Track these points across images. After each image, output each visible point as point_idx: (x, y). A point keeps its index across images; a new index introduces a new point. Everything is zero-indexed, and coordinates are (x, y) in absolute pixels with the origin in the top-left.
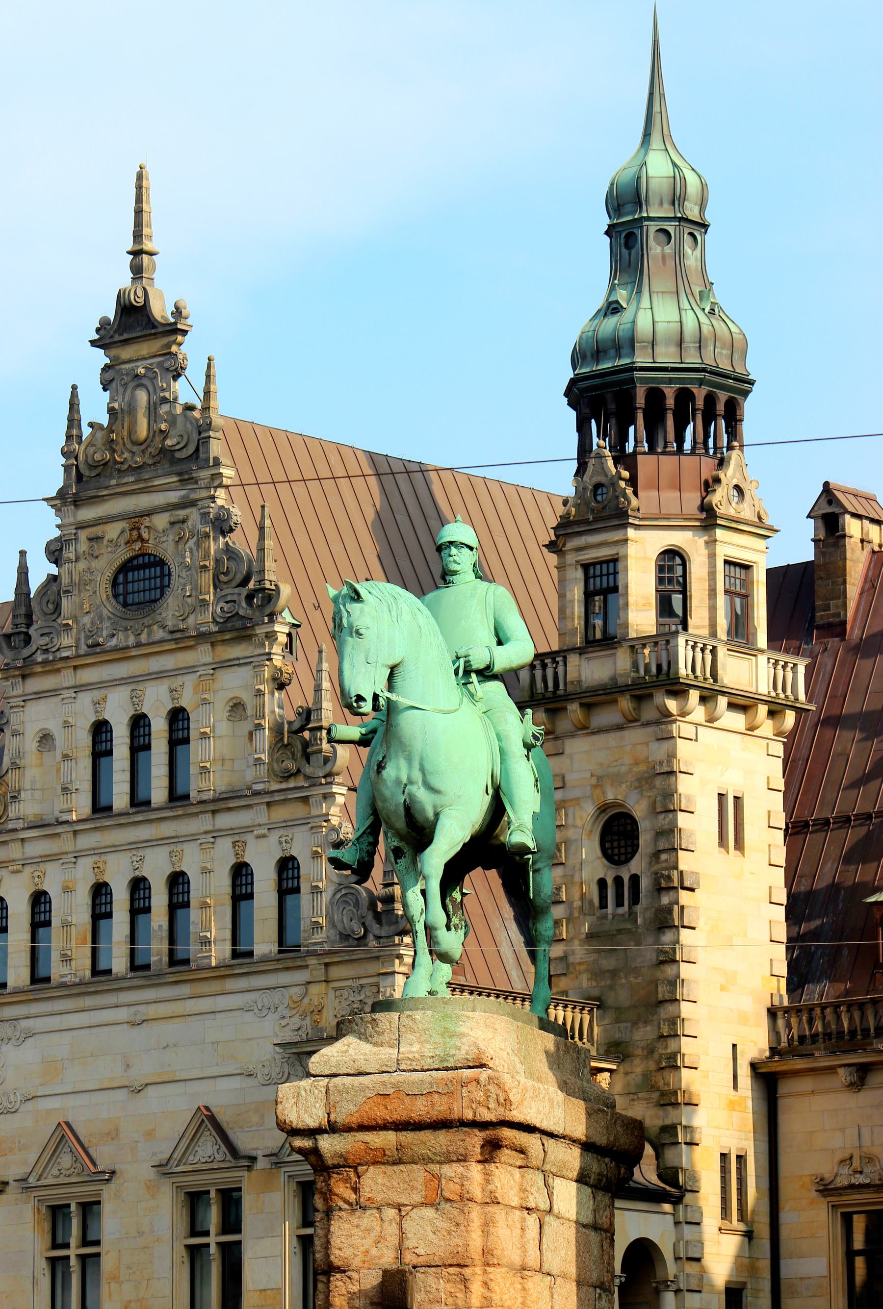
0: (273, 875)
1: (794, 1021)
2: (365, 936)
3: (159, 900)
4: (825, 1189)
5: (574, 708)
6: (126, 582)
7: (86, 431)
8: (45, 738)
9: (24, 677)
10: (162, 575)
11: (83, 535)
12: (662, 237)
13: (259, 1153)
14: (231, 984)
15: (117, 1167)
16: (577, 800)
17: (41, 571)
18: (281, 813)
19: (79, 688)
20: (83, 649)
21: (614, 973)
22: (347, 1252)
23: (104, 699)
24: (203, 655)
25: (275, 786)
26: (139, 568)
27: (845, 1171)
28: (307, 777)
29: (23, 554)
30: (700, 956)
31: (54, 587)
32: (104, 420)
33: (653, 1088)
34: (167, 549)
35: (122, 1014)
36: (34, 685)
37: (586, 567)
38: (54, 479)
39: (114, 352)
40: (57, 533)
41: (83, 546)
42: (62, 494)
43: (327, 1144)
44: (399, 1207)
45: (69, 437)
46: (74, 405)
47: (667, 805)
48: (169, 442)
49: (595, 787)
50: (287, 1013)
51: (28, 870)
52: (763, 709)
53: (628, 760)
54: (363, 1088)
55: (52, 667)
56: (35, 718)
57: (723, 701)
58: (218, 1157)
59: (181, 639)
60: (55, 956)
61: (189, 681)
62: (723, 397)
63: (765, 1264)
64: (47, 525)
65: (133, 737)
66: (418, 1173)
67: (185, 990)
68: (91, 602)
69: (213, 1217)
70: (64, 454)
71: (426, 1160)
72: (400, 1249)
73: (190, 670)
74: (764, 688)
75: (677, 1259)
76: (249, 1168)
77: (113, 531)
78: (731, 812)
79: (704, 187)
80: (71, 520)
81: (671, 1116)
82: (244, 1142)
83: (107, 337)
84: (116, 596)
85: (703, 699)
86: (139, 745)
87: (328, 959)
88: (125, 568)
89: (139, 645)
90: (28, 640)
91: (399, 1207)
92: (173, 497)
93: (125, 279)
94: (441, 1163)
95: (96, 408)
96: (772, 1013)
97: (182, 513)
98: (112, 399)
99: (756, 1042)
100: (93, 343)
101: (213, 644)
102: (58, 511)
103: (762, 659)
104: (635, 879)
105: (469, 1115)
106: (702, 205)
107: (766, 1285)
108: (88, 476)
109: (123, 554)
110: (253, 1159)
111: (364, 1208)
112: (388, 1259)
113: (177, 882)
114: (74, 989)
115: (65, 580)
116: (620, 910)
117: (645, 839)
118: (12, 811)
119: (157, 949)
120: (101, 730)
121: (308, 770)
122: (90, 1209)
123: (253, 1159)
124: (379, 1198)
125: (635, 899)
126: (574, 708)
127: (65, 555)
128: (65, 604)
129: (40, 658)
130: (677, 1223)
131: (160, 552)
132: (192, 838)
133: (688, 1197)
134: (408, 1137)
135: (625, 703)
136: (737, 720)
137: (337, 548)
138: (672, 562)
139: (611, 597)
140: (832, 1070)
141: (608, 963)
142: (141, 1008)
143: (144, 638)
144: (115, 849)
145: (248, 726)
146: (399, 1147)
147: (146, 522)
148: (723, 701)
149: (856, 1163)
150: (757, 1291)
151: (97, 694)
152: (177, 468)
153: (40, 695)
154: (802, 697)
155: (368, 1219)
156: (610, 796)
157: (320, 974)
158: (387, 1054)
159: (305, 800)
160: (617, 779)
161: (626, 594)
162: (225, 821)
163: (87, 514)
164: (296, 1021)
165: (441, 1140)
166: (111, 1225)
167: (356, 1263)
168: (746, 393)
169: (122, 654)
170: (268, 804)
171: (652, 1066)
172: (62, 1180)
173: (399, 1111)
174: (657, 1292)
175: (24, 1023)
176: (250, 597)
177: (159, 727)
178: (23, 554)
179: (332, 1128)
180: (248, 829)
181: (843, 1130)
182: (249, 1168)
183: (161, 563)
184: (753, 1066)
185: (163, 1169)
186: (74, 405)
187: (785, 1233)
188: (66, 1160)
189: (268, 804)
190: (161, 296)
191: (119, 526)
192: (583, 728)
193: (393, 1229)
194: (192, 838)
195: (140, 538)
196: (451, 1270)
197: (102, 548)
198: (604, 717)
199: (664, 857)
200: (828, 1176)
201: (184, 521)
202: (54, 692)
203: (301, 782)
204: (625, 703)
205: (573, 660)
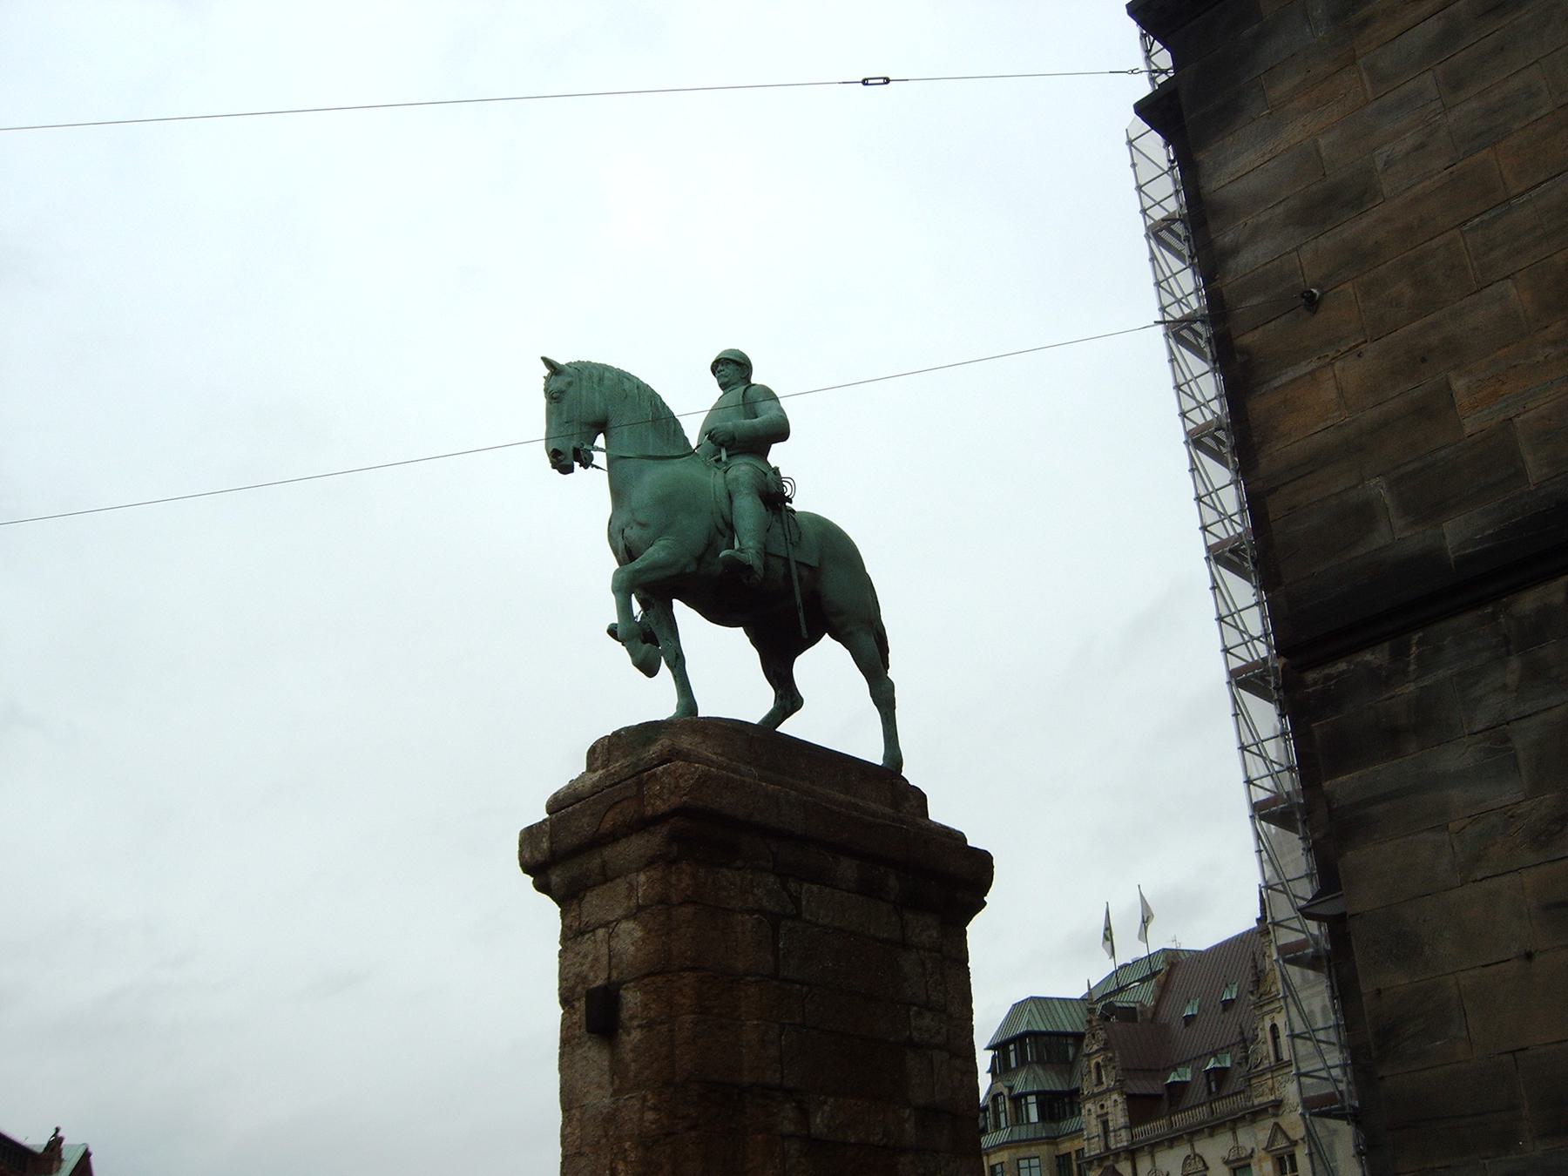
44: (606, 925)
91: (606, 925)
105: (649, 811)
111: (583, 934)
196: (646, 981)
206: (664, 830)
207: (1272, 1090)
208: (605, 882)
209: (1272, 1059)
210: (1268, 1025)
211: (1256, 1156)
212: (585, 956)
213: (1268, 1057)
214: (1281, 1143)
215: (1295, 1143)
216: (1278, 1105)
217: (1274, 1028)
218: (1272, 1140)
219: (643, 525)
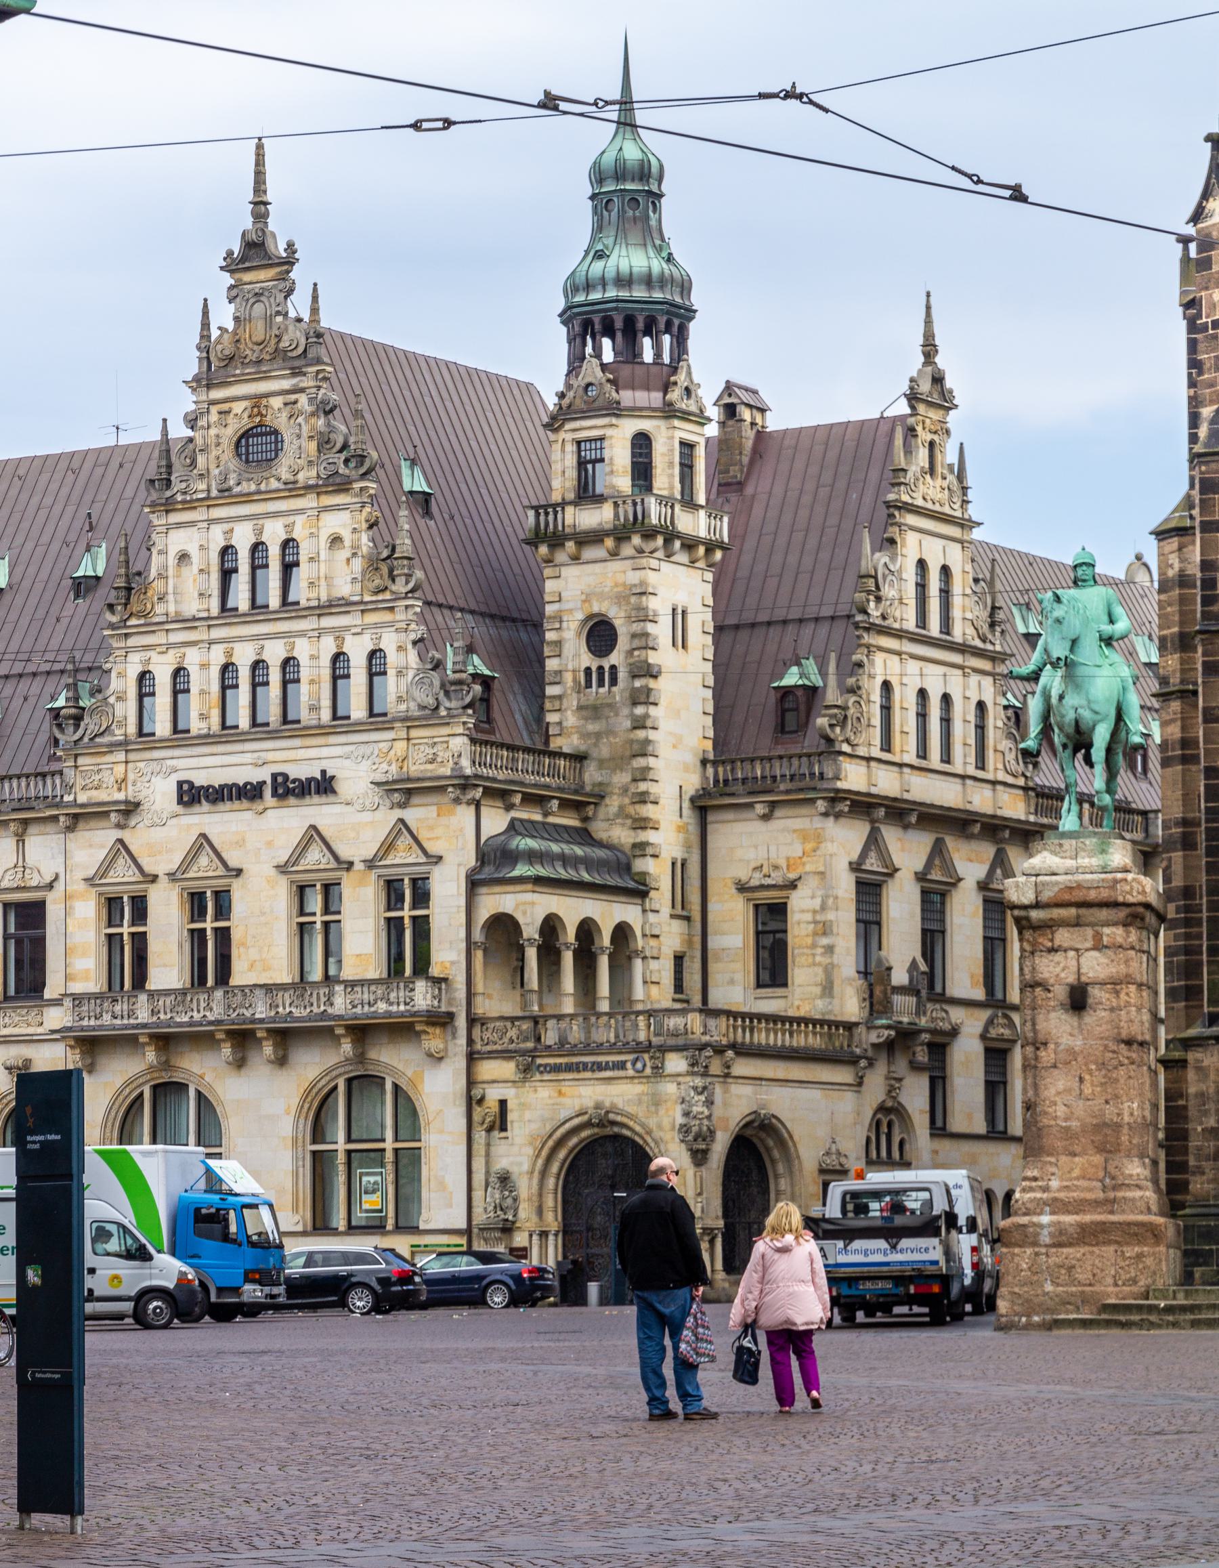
0: (363, 662)
1: (721, 769)
2: (437, 708)
3: (275, 677)
4: (742, 888)
5: (570, 545)
6: (247, 446)
7: (215, 333)
8: (183, 557)
9: (167, 512)
10: (276, 442)
11: (214, 410)
12: (633, 204)
13: (356, 860)
14: (333, 739)
15: (244, 867)
16: (571, 611)
17: (179, 431)
18: (371, 618)
19: (212, 521)
20: (214, 493)
21: (598, 735)
22: (1046, 975)
23: (232, 530)
24: (309, 501)
25: (367, 598)
26: (257, 435)
27: (757, 875)
28: (393, 592)
29: (165, 420)
30: (662, 724)
31: (191, 446)
32: (230, 326)
33: (628, 816)
34: (280, 421)
35: (248, 758)
36: (174, 518)
37: (579, 443)
38: (192, 368)
39: (238, 276)
40: (193, 407)
41: (214, 417)
42: (197, 379)
43: (1035, 914)
44: (1077, 950)
45: (202, 337)
46: (205, 313)
47: (644, 616)
48: (282, 345)
49: (584, 601)
50: (377, 760)
51: (171, 652)
52: (701, 550)
53: (609, 583)
54: (1057, 883)
55: (190, 505)
56: (178, 541)
57: (677, 544)
58: (324, 861)
59: (293, 489)
60: (194, 714)
61: (300, 520)
62: (676, 322)
63: (697, 940)
65: (253, 558)
66: (1089, 932)
67: (297, 742)
68: (219, 459)
69: (315, 902)
70: (199, 348)
71: (1092, 925)
72: (1079, 973)
73: (300, 511)
74: (703, 533)
75: (644, 935)
76: (348, 869)
77: (238, 407)
79: (661, 167)
80: (204, 398)
81: (643, 836)
82: (345, 852)
83: (233, 265)
84: (239, 455)
85: (666, 541)
86: (258, 565)
87: (408, 721)
88: (246, 435)
89: (259, 492)
90: (168, 483)
91: (1077, 950)
92: (286, 384)
93: (248, 223)
95: (224, 316)
96: (704, 762)
97: (293, 397)
98: (237, 310)
99: (693, 783)
100: (222, 268)
101: (318, 494)
102: (194, 390)
103: (702, 513)
104: (613, 668)
105: (1121, 899)
106: (660, 179)
107: (698, 954)
108: (217, 367)
109: (246, 423)
110: (351, 864)
112: (1071, 979)
113: (289, 663)
114: (207, 739)
115: (199, 441)
116: (601, 690)
117: (623, 643)
118: (160, 609)
119: (271, 713)
120: (227, 551)
121: (394, 588)
123: (351, 864)
124: (1065, 945)
125: (614, 681)
126: (570, 545)
127: (200, 423)
128: (201, 460)
129: (179, 498)
130: (644, 911)
131: (275, 424)
132: (302, 634)
133: (652, 894)
134: (1083, 911)
135: (609, 542)
136: (683, 557)
137: (494, 447)
138: (642, 443)
139: (598, 466)
140: (750, 806)
141: (592, 727)
142: (262, 754)
143: (263, 487)
144: (241, 639)
145: (346, 553)
146: (1078, 917)
147: (264, 402)
148: (677, 544)
149: (765, 870)
150: (692, 957)
151: (226, 527)
152: (290, 364)
153: (179, 525)
154: (726, 540)
155: (1058, 957)
156: (596, 609)
157: (403, 734)
158: (1070, 863)
159: (391, 609)
160: (601, 596)
161: (611, 464)
162: (327, 622)
163: (216, 394)
164: (384, 767)
165: (1104, 914)
166: (239, 907)
167: (1052, 981)
168: (691, 319)
169: (246, 498)
170: (363, 611)
171: (627, 801)
172: (201, 874)
173: (1079, 896)
174: (630, 958)
175: (169, 762)
176: (346, 461)
177: (274, 552)
178: (165, 420)
179: (1037, 905)
180: (347, 628)
181: (756, 847)
182: (348, 869)
183: (276, 432)
184: (692, 800)
185: (282, 869)
186: (205, 313)
187: (710, 917)
188: (203, 860)
189: (363, 611)
190: (274, 235)
191: (244, 404)
192: (576, 558)
193: (1074, 963)
194: (302, 634)
195: (260, 414)
197: (230, 419)
198: (589, 553)
199: (636, 653)
200: (744, 879)
201: (295, 402)
202: (192, 524)
203: (387, 596)
204: (609, 542)
205: (570, 510)
207: (121, 783)
208: (1077, 925)
209: (132, 729)
210: (133, 671)
211: (59, 886)
213: (123, 723)
214: (123, 874)
215: (154, 879)
216: (130, 809)
218: (107, 866)
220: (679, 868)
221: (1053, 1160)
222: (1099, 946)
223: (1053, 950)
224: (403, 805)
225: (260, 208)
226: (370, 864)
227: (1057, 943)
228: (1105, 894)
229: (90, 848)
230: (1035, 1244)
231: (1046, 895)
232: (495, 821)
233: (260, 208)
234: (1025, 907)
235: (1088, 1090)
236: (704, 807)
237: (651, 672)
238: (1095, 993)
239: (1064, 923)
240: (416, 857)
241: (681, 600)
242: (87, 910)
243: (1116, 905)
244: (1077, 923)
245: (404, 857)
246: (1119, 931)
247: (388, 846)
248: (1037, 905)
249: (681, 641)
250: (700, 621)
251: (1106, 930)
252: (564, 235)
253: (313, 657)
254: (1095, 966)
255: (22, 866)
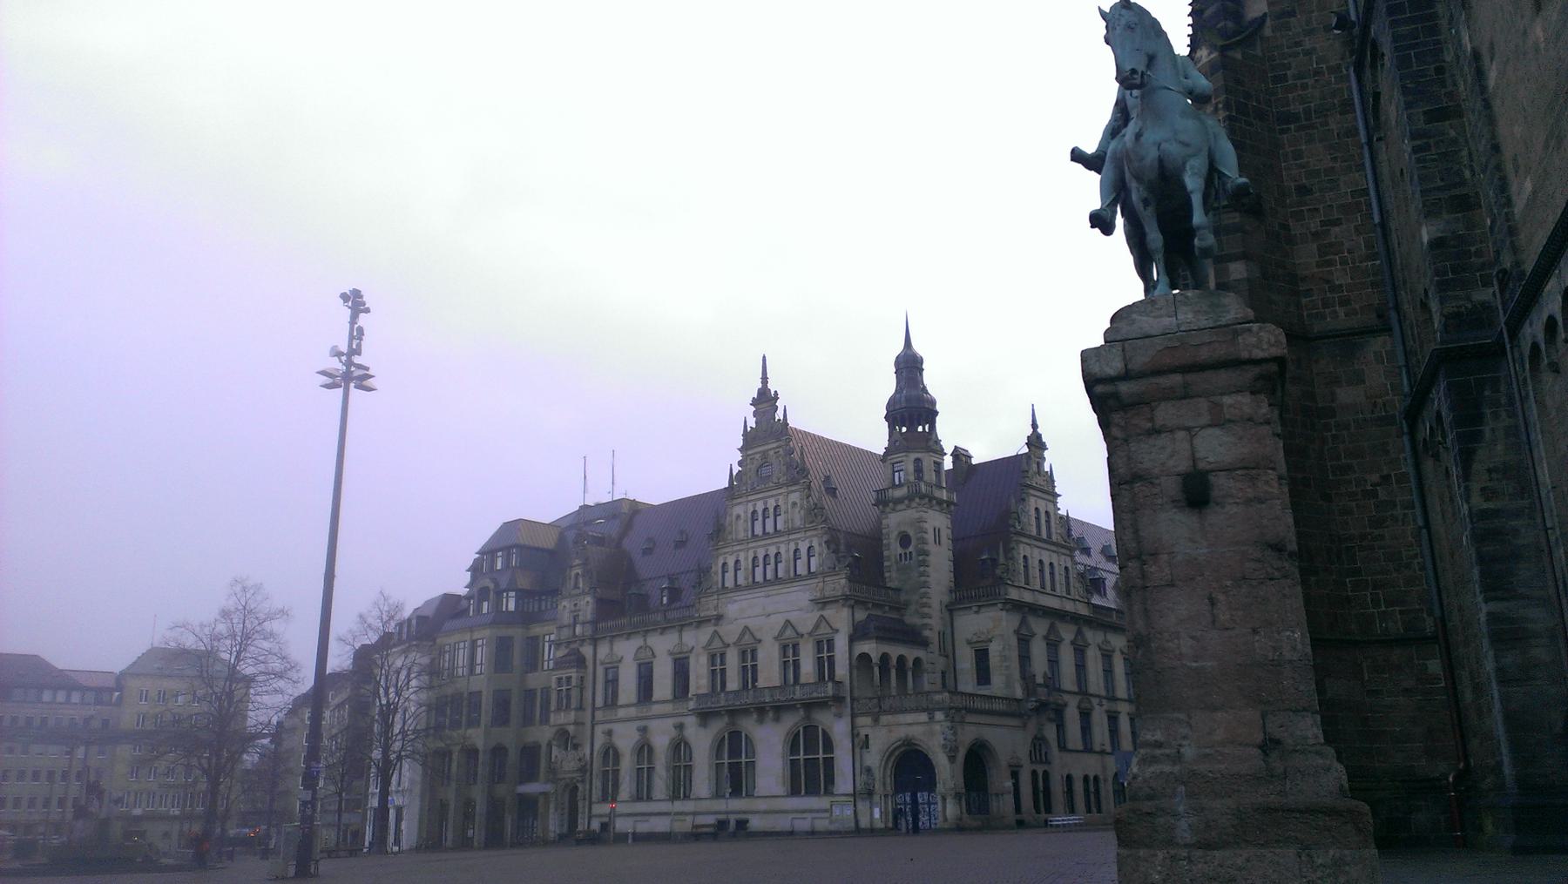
3: (773, 561)
4: (969, 643)
8: (738, 517)
44: (1188, 429)
56: (738, 510)
64: (739, 456)
66: (1203, 404)
78: (937, 532)
81: (926, 621)
82: (800, 630)
83: (755, 402)
91: (1188, 429)
94: (1222, 394)
95: (752, 423)
99: (946, 599)
105: (1245, 355)
112: (1184, 466)
117: (914, 542)
120: (754, 512)
122: (754, 651)
134: (1190, 377)
155: (1162, 440)
165: (1223, 377)
166: (761, 655)
185: (776, 638)
193: (1187, 446)
198: (899, 507)
206: (1256, 370)
207: (716, 607)
210: (721, 562)
212: (1163, 448)
214: (717, 644)
216: (719, 618)
217: (724, 564)
218: (710, 642)
219: (1187, 145)
220: (942, 635)
221: (1182, 716)
222: (1218, 422)
223: (1156, 432)
224: (822, 609)
225: (765, 379)
226: (810, 634)
227: (1159, 422)
228: (1221, 352)
229: (705, 634)
230: (1171, 842)
231: (1140, 361)
232: (861, 615)
233: (765, 379)
234: (1111, 380)
235: (1224, 617)
236: (951, 609)
237: (926, 553)
238: (1221, 483)
239: (1168, 395)
240: (828, 630)
241: (937, 524)
242: (704, 660)
243: (1235, 363)
244: (1186, 395)
245: (824, 629)
246: (1245, 400)
247: (817, 626)
248: (1126, 376)
249: (938, 541)
250: (946, 533)
251: (1227, 400)
252: (886, 385)
253: (786, 551)
254: (1215, 447)
255: (681, 643)
